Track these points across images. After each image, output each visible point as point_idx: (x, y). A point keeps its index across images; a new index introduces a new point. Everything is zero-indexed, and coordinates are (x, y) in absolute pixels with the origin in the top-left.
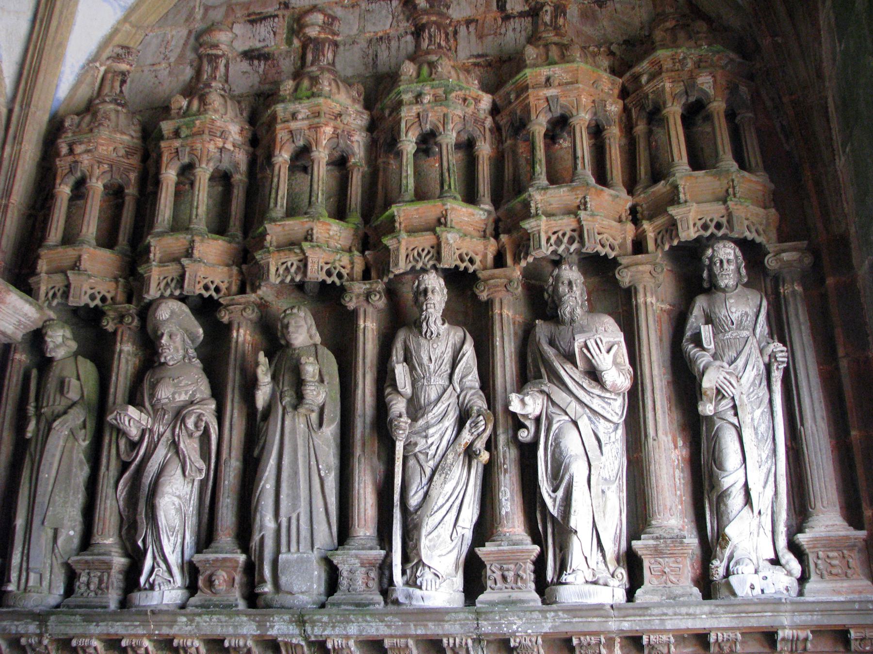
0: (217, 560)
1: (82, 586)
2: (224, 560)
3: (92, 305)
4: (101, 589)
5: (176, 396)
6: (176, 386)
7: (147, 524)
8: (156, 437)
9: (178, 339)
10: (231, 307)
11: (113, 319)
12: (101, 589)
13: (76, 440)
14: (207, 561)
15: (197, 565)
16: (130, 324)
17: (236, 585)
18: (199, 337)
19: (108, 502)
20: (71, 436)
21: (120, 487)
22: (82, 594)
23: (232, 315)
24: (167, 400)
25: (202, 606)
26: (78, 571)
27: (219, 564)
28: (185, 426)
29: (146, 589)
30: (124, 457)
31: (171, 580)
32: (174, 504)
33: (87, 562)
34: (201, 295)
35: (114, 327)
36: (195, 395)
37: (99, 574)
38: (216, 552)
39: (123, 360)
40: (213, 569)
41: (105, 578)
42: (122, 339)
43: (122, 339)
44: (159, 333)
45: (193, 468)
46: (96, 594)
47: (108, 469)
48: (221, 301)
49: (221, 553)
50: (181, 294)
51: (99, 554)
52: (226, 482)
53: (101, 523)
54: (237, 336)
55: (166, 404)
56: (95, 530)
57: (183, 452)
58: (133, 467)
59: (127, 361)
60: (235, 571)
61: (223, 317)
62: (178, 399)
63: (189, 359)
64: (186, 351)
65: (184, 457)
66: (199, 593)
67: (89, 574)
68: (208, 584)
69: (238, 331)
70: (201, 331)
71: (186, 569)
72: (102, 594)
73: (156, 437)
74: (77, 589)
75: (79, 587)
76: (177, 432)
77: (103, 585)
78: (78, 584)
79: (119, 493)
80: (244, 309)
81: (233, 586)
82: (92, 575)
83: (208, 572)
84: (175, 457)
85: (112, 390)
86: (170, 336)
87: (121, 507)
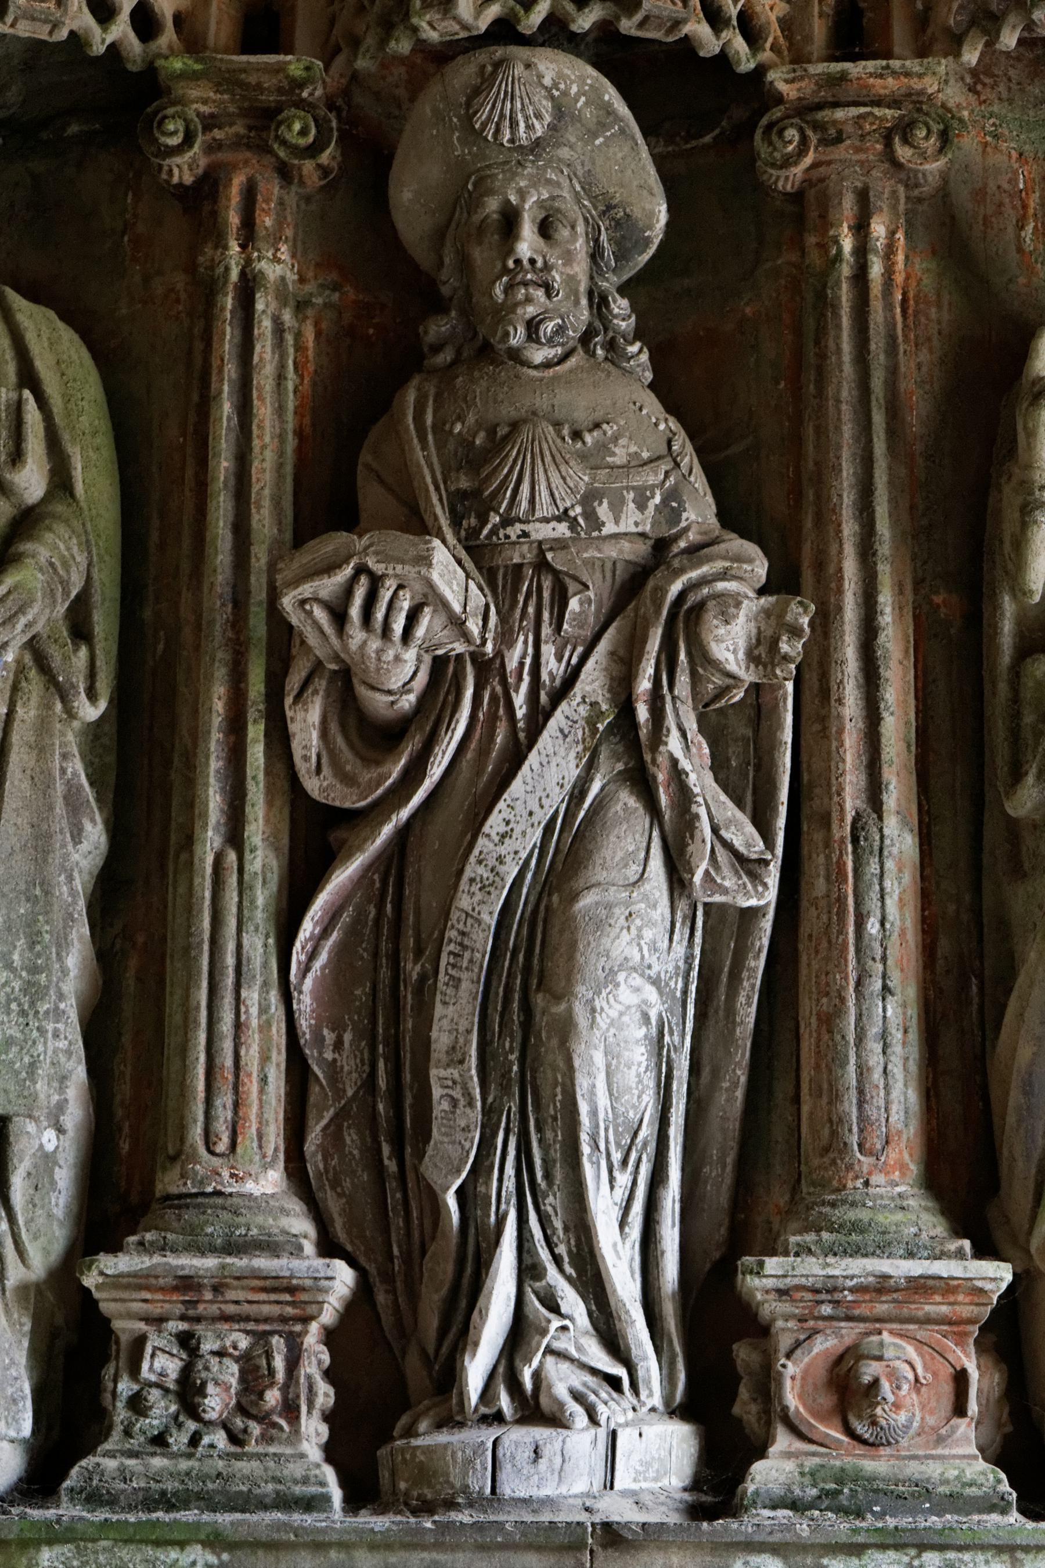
0: (882, 1286)
1: (155, 1394)
2: (920, 1286)
3: (100, 41)
4: (263, 1419)
5: (603, 511)
6: (593, 460)
7: (490, 1114)
8: (520, 699)
9: (580, 246)
10: (840, 114)
11: (210, 123)
12: (263, 1419)
13: (64, 695)
14: (830, 1289)
15: (770, 1307)
16: (313, 150)
17: (973, 1407)
18: (648, 241)
19: (252, 996)
20: (33, 674)
21: (308, 928)
22: (160, 1441)
23: (841, 152)
24: (562, 529)
25: (829, 1501)
26: (125, 1327)
27: (882, 1308)
28: (700, 657)
29: (498, 1418)
30: (312, 786)
31: (621, 1372)
32: (646, 1018)
33: (187, 1283)
34: (687, 44)
35: (203, 162)
36: (675, 516)
37: (244, 1343)
38: (858, 1251)
39: (265, 325)
40: (850, 1332)
41: (279, 1363)
42: (248, 224)
43: (248, 224)
44: (492, 205)
45: (722, 855)
46: (235, 1438)
47: (235, 837)
48: (778, 79)
49: (883, 1249)
50: (606, 30)
51: (232, 1248)
52: (873, 927)
53: (224, 1100)
54: (862, 251)
55: (559, 545)
56: (197, 1132)
57: (677, 774)
58: (387, 830)
59: (279, 329)
60: (960, 1339)
61: (788, 162)
62: (609, 528)
63: (611, 346)
64: (599, 302)
65: (684, 796)
66: (783, 1441)
67: (187, 1341)
68: (827, 1400)
69: (861, 228)
70: (663, 217)
71: (669, 1311)
72: (266, 1438)
73: (520, 699)
74: (121, 1414)
75: (137, 1404)
76: (644, 685)
77: (273, 1397)
78: (125, 1387)
79: (298, 956)
80: (904, 130)
81: (960, 1409)
82: (208, 1346)
83: (825, 1345)
84: (627, 800)
85: (223, 465)
86: (545, 229)
87: (304, 1024)
